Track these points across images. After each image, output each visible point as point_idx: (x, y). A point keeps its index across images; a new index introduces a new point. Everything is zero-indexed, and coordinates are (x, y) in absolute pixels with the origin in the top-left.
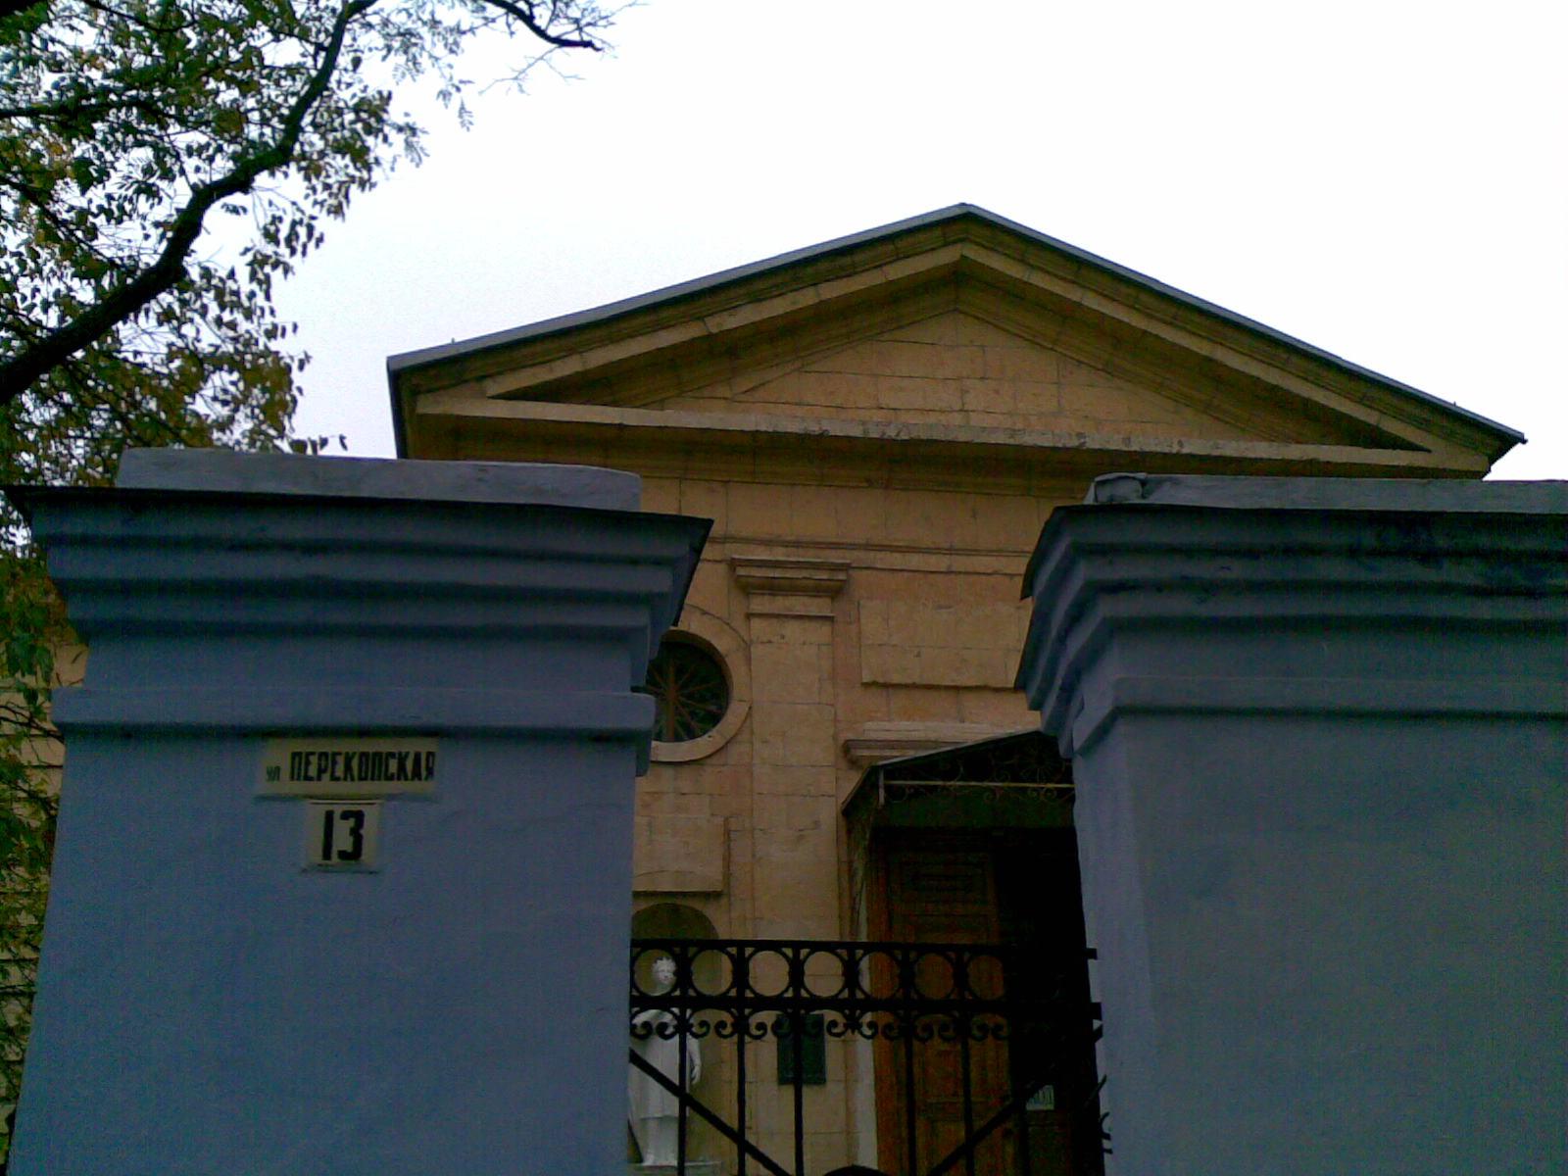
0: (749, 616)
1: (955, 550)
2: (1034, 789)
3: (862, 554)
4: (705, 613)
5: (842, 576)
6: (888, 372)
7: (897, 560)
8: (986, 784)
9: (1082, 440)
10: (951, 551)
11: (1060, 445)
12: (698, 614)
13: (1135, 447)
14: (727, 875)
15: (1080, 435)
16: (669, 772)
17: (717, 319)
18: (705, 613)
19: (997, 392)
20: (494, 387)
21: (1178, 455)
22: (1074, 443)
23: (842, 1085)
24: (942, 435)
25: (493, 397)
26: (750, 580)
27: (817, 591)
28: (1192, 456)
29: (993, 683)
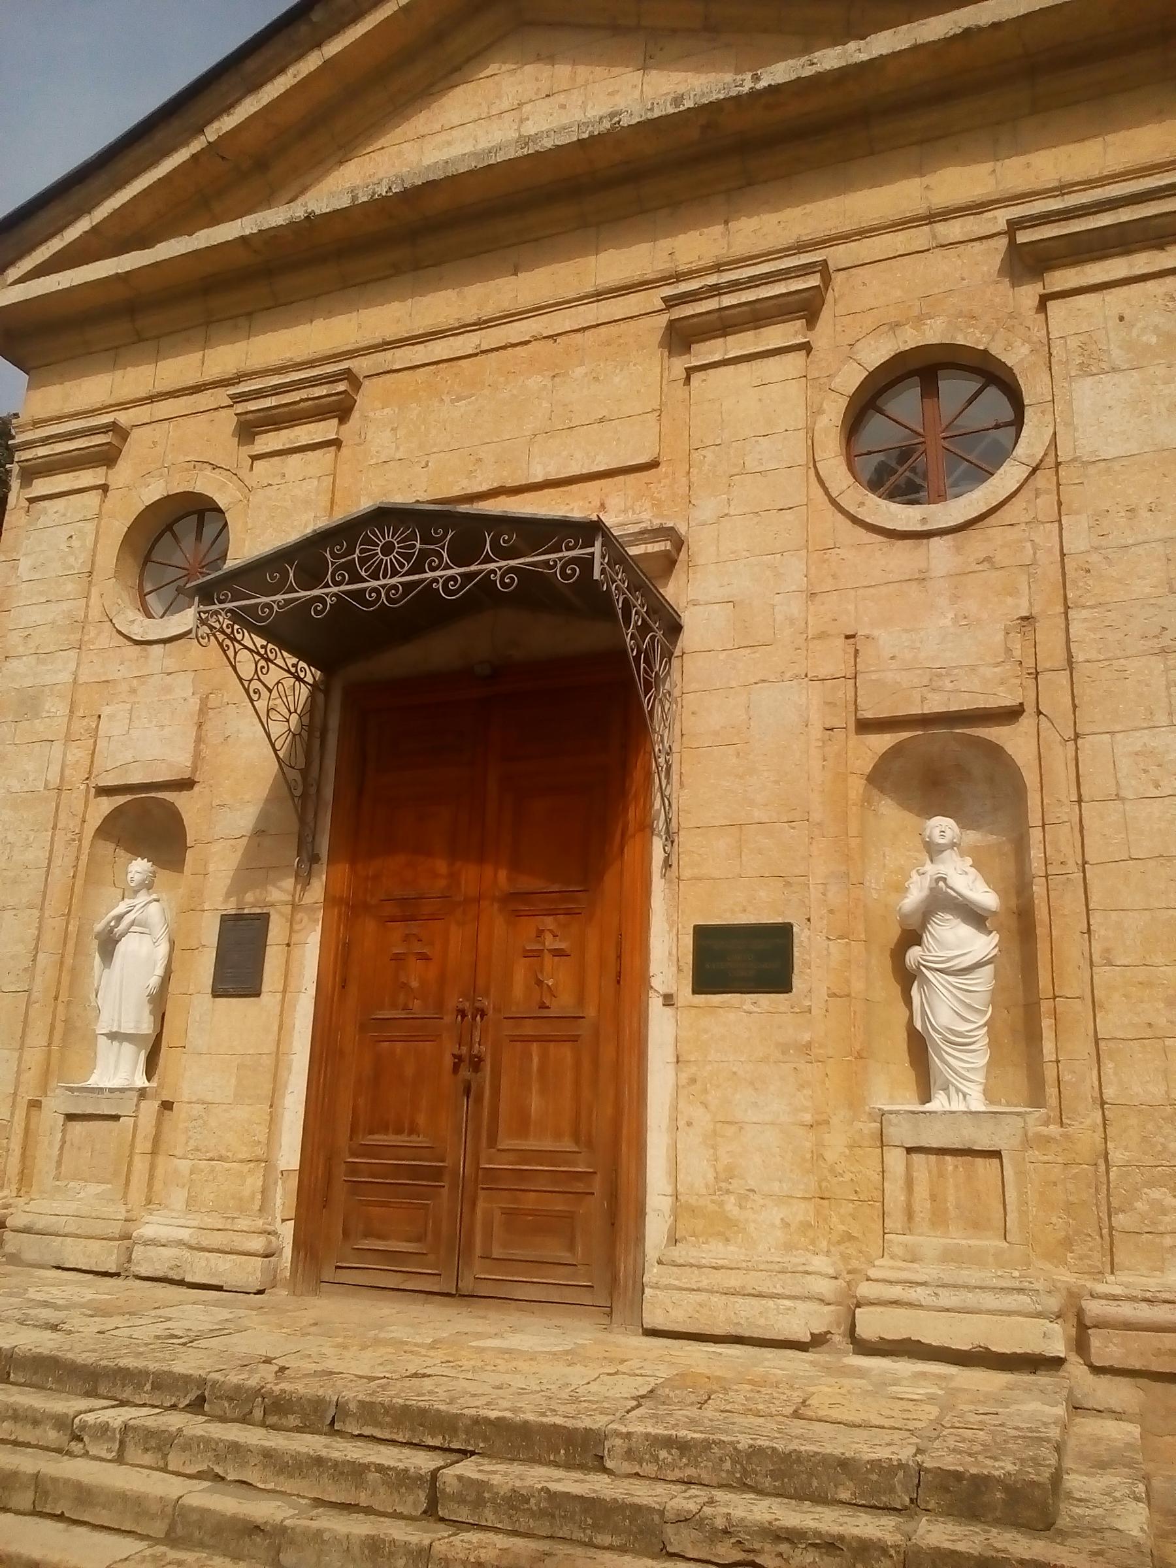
0: (254, 458)
1: (486, 322)
2: (375, 590)
3: (380, 356)
4: (215, 467)
5: (341, 387)
6: (438, 127)
7: (419, 354)
8: (316, 592)
9: (617, 119)
10: (482, 324)
11: (586, 136)
12: (208, 471)
13: (689, 104)
14: (197, 756)
15: (612, 115)
16: (157, 649)
17: (216, 125)
18: (215, 467)
19: (563, 107)
20: (13, 273)
21: (754, 94)
22: (607, 125)
23: (279, 996)
24: (440, 173)
25: (12, 284)
26: (249, 416)
27: (318, 413)
28: (772, 89)
29: (510, 483)
